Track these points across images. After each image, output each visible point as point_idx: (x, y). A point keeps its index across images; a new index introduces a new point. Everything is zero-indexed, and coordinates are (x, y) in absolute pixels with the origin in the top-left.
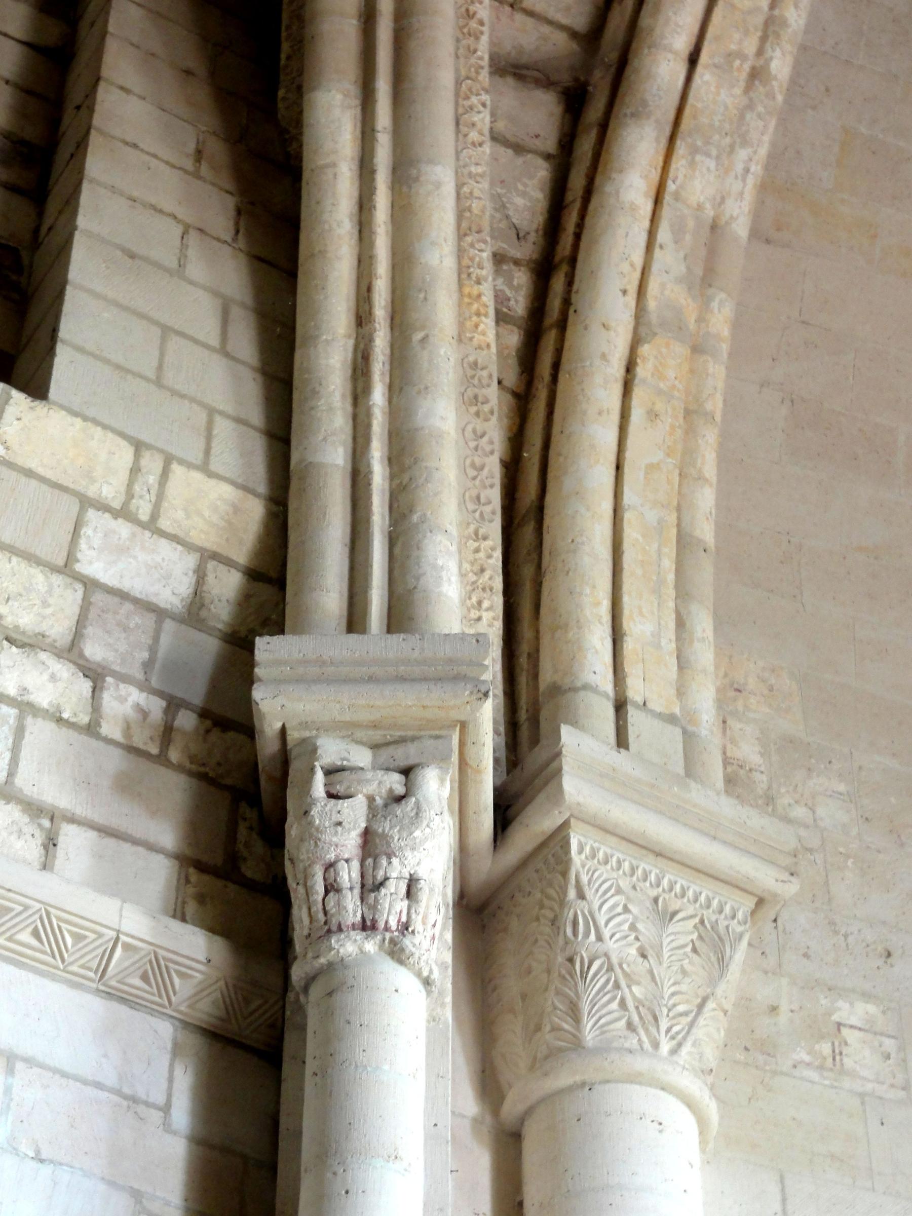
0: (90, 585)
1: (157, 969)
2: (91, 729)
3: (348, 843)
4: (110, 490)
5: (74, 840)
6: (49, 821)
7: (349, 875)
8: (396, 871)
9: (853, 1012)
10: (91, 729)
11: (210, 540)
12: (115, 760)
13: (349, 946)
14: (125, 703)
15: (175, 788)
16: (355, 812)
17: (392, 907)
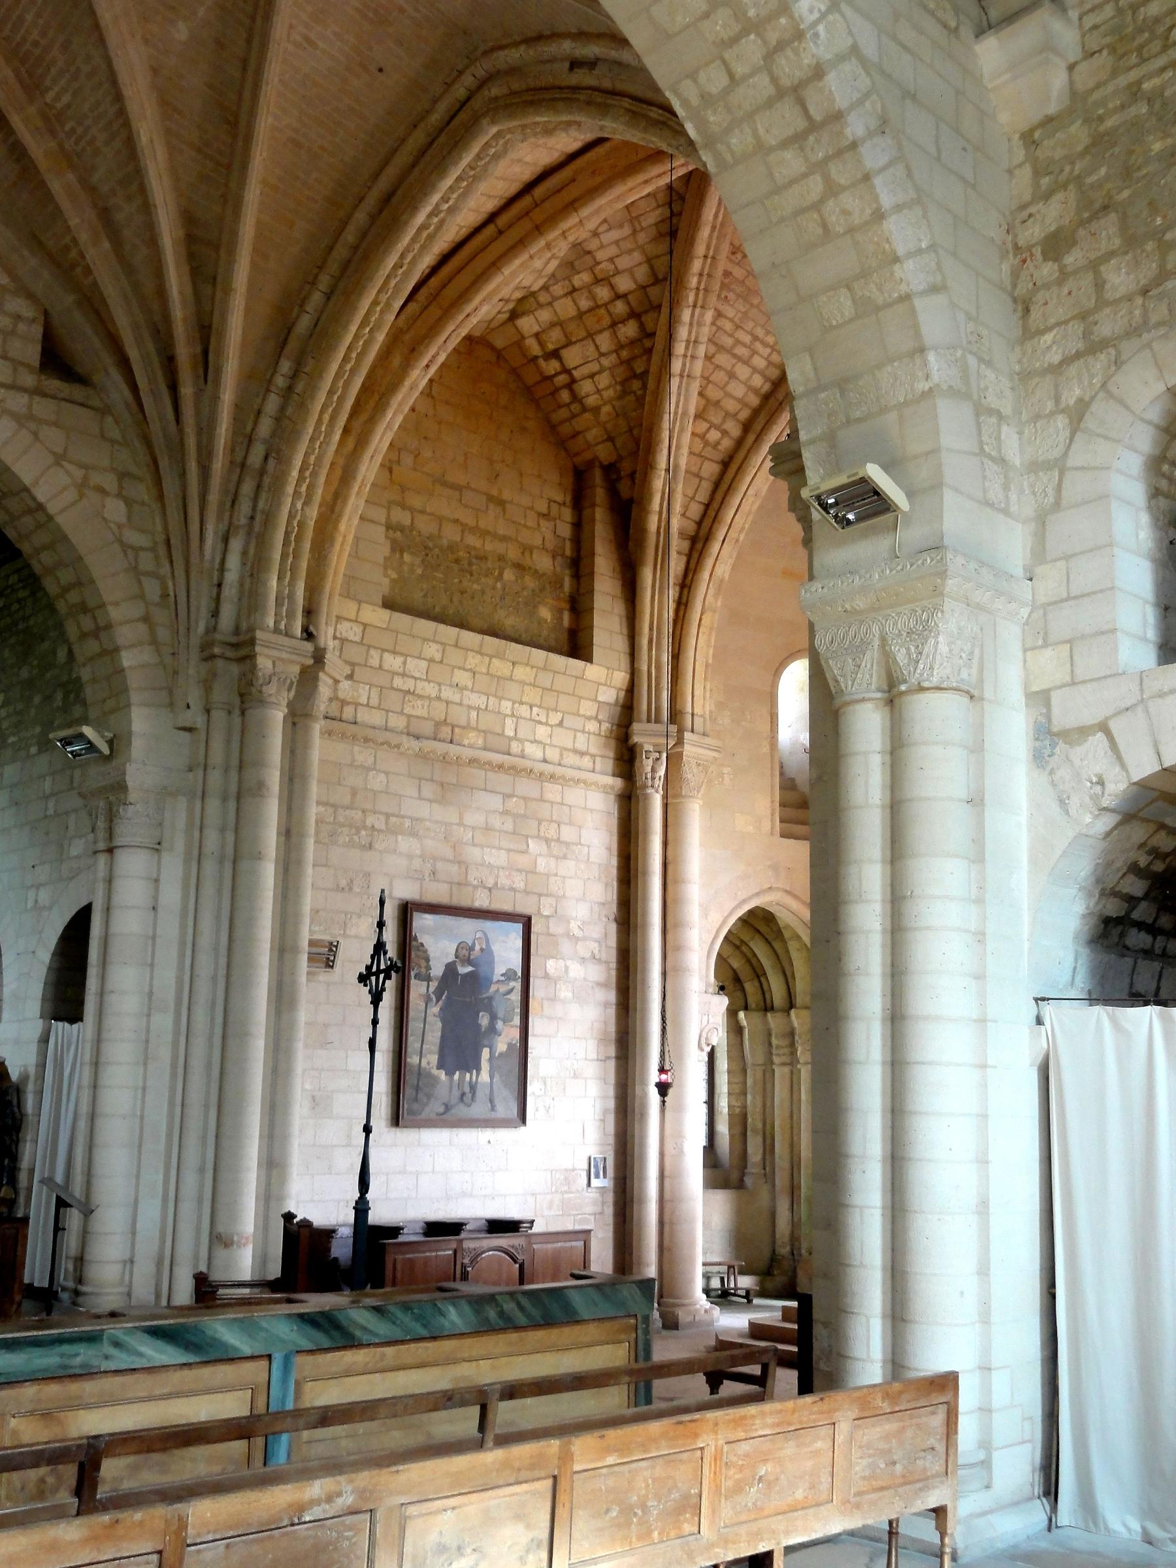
0: (600, 702)
1: (612, 787)
2: (599, 735)
3: (649, 769)
4: (603, 681)
5: (598, 759)
6: (593, 756)
7: (649, 776)
8: (657, 776)
9: (726, 770)
10: (599, 735)
11: (619, 685)
12: (603, 740)
13: (650, 791)
14: (606, 726)
15: (613, 743)
16: (650, 762)
17: (657, 782)
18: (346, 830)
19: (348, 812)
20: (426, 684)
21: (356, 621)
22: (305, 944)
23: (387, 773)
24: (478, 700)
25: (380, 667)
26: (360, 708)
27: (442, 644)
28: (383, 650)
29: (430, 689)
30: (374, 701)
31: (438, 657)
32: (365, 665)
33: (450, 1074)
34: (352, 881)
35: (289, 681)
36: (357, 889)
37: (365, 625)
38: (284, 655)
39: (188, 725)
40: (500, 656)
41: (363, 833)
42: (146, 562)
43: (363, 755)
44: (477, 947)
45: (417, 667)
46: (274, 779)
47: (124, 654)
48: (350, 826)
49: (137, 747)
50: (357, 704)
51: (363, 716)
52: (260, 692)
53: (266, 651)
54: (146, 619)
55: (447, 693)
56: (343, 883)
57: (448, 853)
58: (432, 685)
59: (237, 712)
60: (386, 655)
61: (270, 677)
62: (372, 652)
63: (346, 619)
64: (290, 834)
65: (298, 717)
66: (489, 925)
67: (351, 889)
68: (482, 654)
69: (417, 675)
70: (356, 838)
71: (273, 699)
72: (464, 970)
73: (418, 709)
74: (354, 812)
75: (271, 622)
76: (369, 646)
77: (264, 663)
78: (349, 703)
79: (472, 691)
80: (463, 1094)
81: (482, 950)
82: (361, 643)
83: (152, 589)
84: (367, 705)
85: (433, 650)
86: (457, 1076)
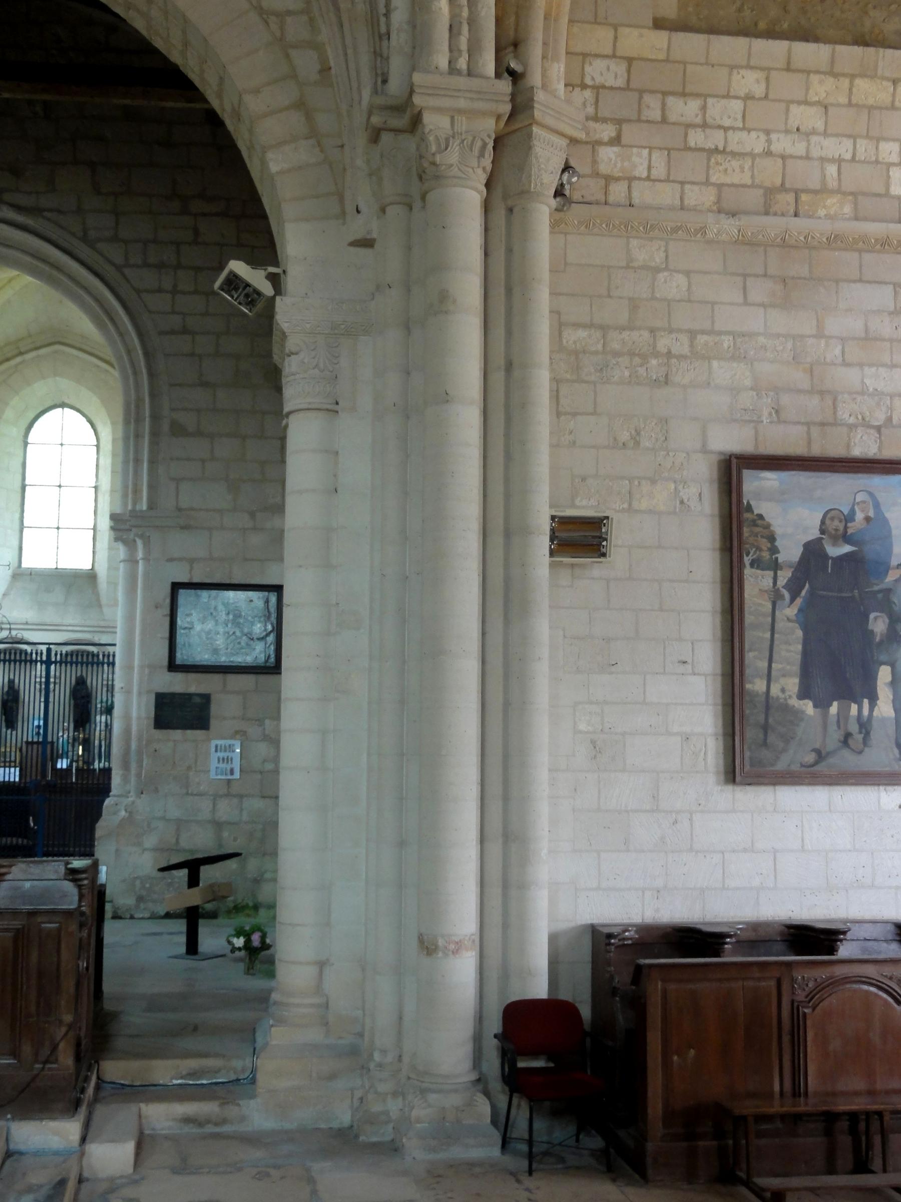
18: (624, 361)
19: (625, 334)
20: (744, 134)
21: (614, 56)
22: (545, 526)
23: (687, 273)
24: (833, 147)
25: (664, 120)
26: (635, 184)
27: (762, 69)
28: (665, 94)
29: (755, 142)
30: (659, 171)
31: (759, 90)
32: (639, 120)
33: (822, 704)
34: (638, 433)
35: (479, 144)
36: (646, 443)
37: (630, 60)
38: (462, 103)
39: (359, 236)
40: (869, 73)
41: (654, 362)
42: (296, 29)
43: (645, 252)
44: (859, 516)
45: (725, 111)
46: (468, 287)
47: (270, 155)
48: (632, 354)
49: (296, 275)
50: (631, 179)
51: (642, 194)
52: (434, 164)
53: (432, 102)
54: (300, 105)
55: (782, 144)
56: (625, 436)
57: (800, 378)
58: (754, 134)
59: (417, 204)
60: (671, 101)
61: (447, 140)
62: (648, 99)
63: (597, 56)
64: (505, 369)
65: (504, 193)
66: (877, 482)
67: (637, 443)
68: (836, 75)
69: (727, 123)
70: (642, 371)
71: (455, 171)
72: (835, 551)
73: (733, 173)
74: (635, 335)
75: (442, 61)
76: (641, 92)
77: (435, 123)
78: (618, 179)
79: (825, 134)
80: (848, 735)
81: (868, 519)
82: (628, 88)
83: (306, 63)
84: (648, 178)
85: (749, 82)
86: (834, 708)
